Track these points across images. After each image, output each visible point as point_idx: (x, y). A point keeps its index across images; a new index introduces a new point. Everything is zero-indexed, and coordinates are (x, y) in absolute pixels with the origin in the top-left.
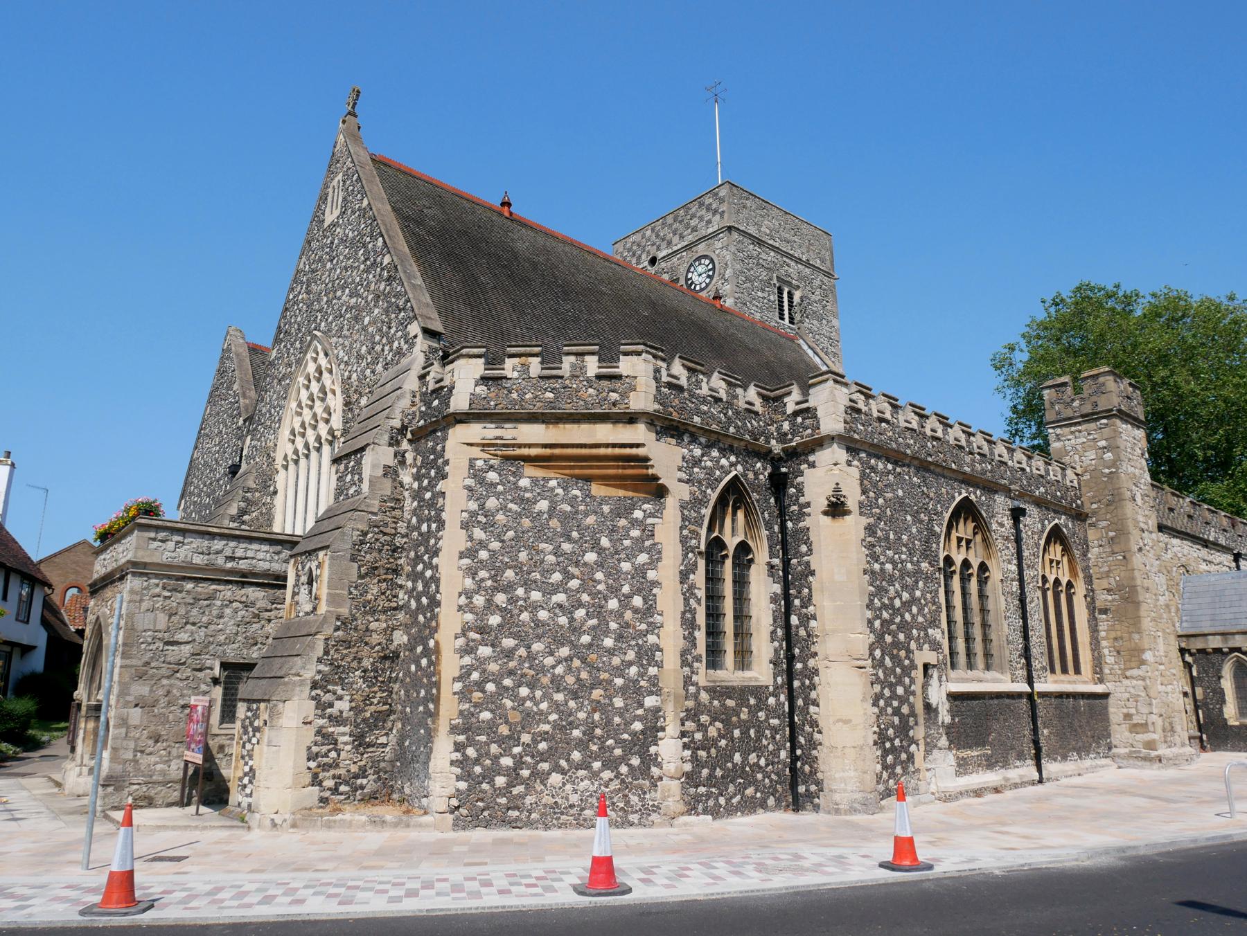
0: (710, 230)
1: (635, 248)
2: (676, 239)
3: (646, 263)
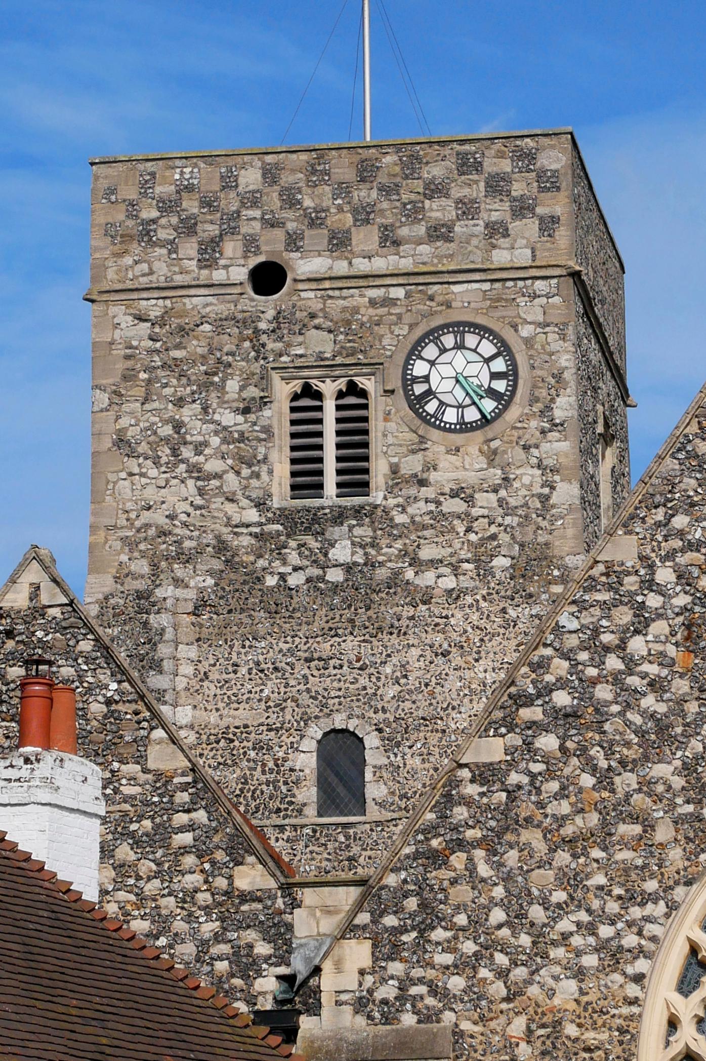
0: (500, 257)
1: (191, 206)
2: (365, 238)
3: (240, 274)
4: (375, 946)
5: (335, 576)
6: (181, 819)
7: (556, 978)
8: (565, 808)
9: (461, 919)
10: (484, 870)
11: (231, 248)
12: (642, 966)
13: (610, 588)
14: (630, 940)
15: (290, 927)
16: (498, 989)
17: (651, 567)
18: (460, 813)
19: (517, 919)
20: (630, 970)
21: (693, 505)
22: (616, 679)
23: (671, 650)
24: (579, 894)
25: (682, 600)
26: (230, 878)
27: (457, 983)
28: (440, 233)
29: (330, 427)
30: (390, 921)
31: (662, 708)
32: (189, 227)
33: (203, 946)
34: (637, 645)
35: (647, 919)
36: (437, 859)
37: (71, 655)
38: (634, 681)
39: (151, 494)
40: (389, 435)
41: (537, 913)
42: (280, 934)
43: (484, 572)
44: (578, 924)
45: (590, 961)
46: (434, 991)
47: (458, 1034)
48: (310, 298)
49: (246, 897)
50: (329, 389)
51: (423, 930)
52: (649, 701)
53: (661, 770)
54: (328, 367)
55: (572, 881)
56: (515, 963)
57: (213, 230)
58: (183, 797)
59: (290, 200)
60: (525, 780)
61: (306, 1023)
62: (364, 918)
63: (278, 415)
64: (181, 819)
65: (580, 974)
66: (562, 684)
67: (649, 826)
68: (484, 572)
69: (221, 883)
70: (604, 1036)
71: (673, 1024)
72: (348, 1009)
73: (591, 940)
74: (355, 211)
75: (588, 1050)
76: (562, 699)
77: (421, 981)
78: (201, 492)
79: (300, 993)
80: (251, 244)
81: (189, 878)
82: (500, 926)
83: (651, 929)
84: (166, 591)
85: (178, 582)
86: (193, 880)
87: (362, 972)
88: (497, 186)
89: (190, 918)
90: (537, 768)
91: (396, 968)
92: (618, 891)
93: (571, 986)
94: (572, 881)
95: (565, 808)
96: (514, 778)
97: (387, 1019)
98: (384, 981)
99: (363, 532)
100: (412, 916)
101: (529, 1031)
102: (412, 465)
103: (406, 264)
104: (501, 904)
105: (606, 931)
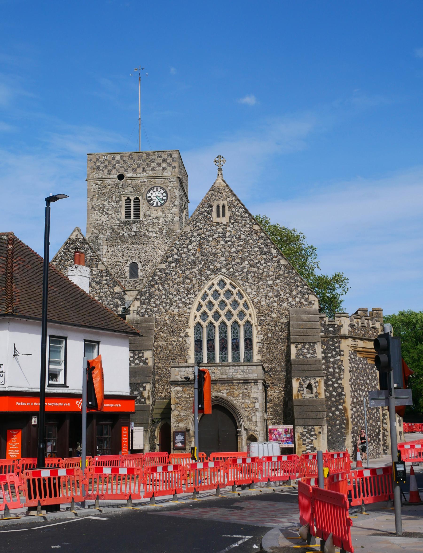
0: (165, 174)
1: (106, 163)
3: (116, 176)
4: (140, 302)
5: (133, 234)
6: (104, 278)
7: (174, 308)
8: (176, 277)
9: (157, 297)
10: (161, 288)
11: (114, 171)
12: (190, 306)
13: (185, 236)
14: (188, 301)
15: (125, 299)
16: (163, 310)
17: (193, 232)
18: (157, 278)
19: (167, 297)
20: (188, 307)
21: (201, 221)
22: (186, 253)
23: (196, 248)
24: (179, 293)
25: (198, 239)
26: (113, 289)
27: (156, 309)
28: (154, 169)
29: (132, 206)
30: (143, 298)
31: (194, 259)
32: (106, 167)
33: (108, 302)
34: (190, 247)
35: (191, 298)
36: (152, 286)
37: (83, 248)
38: (189, 254)
39: (98, 218)
40: (143, 206)
41: (171, 296)
42: (123, 300)
43: (161, 233)
44: (178, 298)
45: (180, 305)
46: (151, 311)
47: (156, 319)
48: (129, 181)
49: (116, 293)
50: (132, 198)
51: (150, 299)
52: (192, 257)
53: (194, 270)
54: (132, 194)
55: (177, 290)
56: (166, 305)
57: (110, 168)
58: (105, 274)
59: (125, 162)
60: (169, 272)
61: (128, 316)
62: (138, 297)
63: (123, 203)
64: (104, 278)
65: (179, 308)
66: (176, 254)
67: (192, 280)
68: (161, 233)
69: (112, 290)
70: (183, 319)
71: (196, 317)
72: (135, 314)
73: (181, 301)
74: (138, 165)
75: (180, 321)
76: (176, 257)
77: (149, 309)
78: (108, 217)
79: (126, 311)
80: (118, 171)
81: (106, 289)
82: (164, 299)
83: (192, 299)
84: (101, 236)
85: (103, 234)
86: (106, 290)
87: (138, 307)
88: (164, 160)
89: (106, 297)
90: (171, 269)
91: (144, 306)
92: (186, 292)
93: (177, 310)
94: (177, 290)
95: (176, 277)
96: (167, 271)
97: (143, 316)
98: (142, 309)
99: (139, 225)
100: (147, 297)
101: (169, 318)
102: (148, 213)
103: (147, 175)
104: (164, 295)
105: (183, 300)
